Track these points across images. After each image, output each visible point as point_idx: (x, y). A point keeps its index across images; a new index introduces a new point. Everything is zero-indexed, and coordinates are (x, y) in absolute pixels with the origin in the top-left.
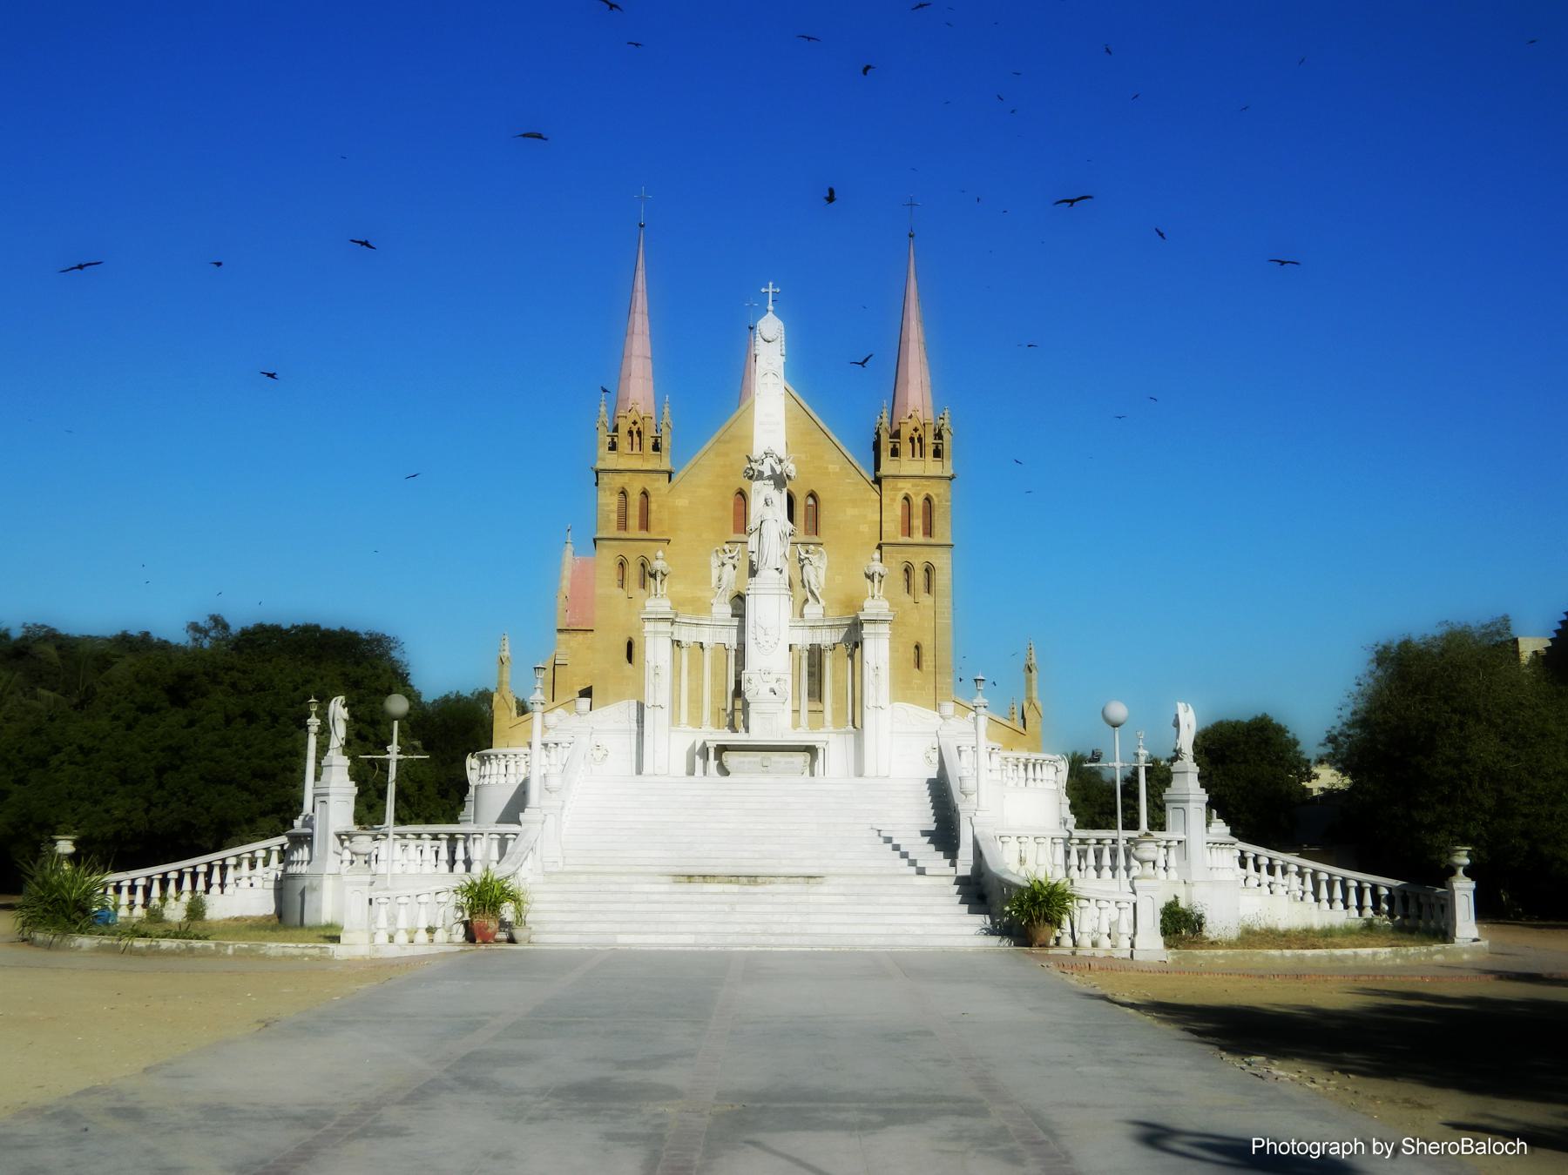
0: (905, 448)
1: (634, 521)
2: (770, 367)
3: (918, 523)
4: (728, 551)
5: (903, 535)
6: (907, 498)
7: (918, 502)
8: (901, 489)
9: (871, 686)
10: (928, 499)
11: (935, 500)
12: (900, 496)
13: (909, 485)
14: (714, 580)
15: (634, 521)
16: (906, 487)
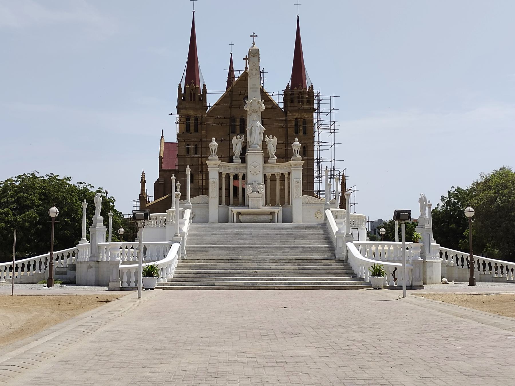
8: (295, 115)
9: (295, 189)
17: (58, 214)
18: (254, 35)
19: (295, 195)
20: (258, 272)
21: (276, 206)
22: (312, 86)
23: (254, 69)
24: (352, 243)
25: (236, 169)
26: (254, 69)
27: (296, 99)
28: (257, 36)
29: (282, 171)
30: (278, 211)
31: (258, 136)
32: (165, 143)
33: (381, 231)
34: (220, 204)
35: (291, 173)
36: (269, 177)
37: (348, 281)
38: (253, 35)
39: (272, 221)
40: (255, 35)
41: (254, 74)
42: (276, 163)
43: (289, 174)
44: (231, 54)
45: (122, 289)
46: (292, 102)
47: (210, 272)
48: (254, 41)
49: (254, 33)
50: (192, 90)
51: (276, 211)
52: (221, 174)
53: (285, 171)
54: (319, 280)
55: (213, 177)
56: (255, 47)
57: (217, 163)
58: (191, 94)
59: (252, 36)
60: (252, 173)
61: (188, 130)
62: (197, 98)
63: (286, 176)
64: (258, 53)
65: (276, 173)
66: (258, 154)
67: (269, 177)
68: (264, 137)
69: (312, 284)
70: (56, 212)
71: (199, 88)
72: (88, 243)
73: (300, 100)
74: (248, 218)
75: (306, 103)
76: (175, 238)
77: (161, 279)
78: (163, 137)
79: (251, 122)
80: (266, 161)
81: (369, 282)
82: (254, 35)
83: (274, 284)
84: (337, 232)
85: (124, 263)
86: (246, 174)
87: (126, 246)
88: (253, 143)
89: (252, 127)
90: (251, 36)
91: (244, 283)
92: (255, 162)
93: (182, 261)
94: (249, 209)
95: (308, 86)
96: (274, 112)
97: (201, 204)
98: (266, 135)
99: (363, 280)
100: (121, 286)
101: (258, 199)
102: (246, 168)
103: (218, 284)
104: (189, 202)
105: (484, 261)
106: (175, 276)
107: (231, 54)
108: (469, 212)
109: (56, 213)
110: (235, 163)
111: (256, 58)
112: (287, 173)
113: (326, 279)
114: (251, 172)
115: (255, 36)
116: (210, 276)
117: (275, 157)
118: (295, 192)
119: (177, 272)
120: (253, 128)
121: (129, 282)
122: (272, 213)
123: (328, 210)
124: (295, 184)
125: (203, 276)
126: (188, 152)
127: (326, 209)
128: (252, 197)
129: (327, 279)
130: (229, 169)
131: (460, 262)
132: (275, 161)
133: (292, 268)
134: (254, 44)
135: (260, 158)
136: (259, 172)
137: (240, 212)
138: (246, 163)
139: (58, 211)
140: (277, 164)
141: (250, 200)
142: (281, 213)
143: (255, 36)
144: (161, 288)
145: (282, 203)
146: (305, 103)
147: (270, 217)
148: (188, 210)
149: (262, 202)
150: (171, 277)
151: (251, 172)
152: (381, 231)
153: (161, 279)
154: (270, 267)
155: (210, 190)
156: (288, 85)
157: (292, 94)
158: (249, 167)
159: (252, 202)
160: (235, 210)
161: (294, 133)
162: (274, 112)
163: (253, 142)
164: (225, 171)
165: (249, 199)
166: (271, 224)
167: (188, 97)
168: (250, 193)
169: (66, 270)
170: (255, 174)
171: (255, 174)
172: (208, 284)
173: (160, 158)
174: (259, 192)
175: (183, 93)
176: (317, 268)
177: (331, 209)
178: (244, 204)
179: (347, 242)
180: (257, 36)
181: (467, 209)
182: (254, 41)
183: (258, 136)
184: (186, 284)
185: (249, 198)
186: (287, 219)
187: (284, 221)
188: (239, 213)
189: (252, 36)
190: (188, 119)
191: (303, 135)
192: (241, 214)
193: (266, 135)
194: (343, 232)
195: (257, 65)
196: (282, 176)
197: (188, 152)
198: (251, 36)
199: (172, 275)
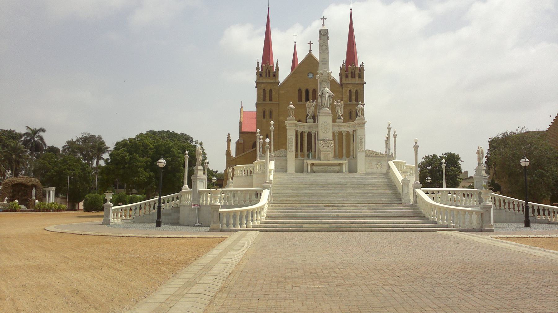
0: (350, 75)
1: (268, 98)
2: (324, 44)
3: (353, 97)
4: (312, 102)
5: (349, 101)
6: (350, 91)
7: (354, 91)
8: (349, 87)
9: (359, 144)
10: (357, 91)
11: (359, 91)
12: (348, 90)
13: (351, 86)
14: (307, 111)
15: (268, 98)
16: (350, 87)
17: (165, 164)
18: (324, 18)
19: (359, 149)
20: (339, 215)
21: (342, 158)
22: (363, 64)
23: (324, 46)
24: (420, 189)
25: (310, 127)
26: (324, 46)
27: (350, 75)
28: (326, 19)
29: (347, 129)
30: (344, 162)
31: (328, 101)
32: (244, 112)
33: (427, 179)
34: (297, 156)
35: (355, 131)
36: (336, 134)
37: (420, 224)
38: (323, 18)
39: (340, 171)
40: (324, 18)
41: (324, 49)
42: (343, 122)
43: (354, 131)
44: (295, 42)
45: (222, 230)
46: (347, 76)
47: (297, 215)
48: (323, 23)
49: (324, 17)
50: (268, 68)
51: (343, 162)
52: (297, 132)
53: (350, 129)
54: (395, 223)
55: (291, 135)
56: (325, 27)
57: (294, 123)
58: (266, 71)
59: (322, 19)
60: (323, 131)
61: (264, 99)
62: (271, 75)
63: (351, 134)
64: (327, 32)
66: (328, 115)
67: (336, 134)
68: (333, 102)
69: (390, 226)
70: (164, 163)
71: (273, 66)
72: (189, 190)
73: (353, 75)
75: (358, 78)
76: (265, 185)
77: (255, 221)
78: (242, 107)
79: (322, 89)
80: (334, 121)
81: (441, 225)
82: (324, 18)
83: (356, 227)
84: (403, 180)
85: (224, 207)
86: (318, 132)
88: (324, 106)
89: (323, 93)
90: (321, 19)
91: (329, 225)
92: (325, 122)
93: (271, 205)
95: (359, 63)
96: (333, 85)
98: (335, 100)
99: (435, 223)
100: (221, 228)
101: (328, 152)
102: (318, 127)
103: (306, 226)
104: (273, 155)
105: (538, 207)
106: (267, 219)
107: (295, 42)
108: (525, 163)
109: (163, 164)
110: (309, 122)
111: (326, 37)
112: (352, 131)
115: (325, 19)
116: (298, 219)
117: (342, 117)
118: (359, 147)
119: (268, 215)
120: (324, 94)
121: (228, 225)
122: (340, 165)
123: (390, 161)
124: (359, 140)
125: (291, 219)
126: (264, 117)
127: (388, 161)
128: (324, 151)
130: (304, 128)
131: (516, 208)
132: (342, 121)
133: (368, 212)
134: (323, 25)
135: (330, 119)
137: (313, 163)
138: (317, 123)
139: (165, 162)
140: (344, 123)
141: (322, 154)
142: (347, 164)
143: (325, 19)
144: (256, 230)
145: (348, 156)
146: (357, 78)
147: (337, 168)
148: (272, 161)
149: (331, 155)
150: (263, 219)
151: (322, 130)
152: (427, 179)
153: (256, 221)
154: (350, 211)
155: (289, 145)
156: (344, 64)
157: (347, 71)
158: (320, 125)
159: (323, 155)
160: (310, 162)
161: (348, 101)
162: (333, 85)
163: (324, 105)
164: (300, 130)
165: (320, 153)
166: (338, 174)
167: (264, 74)
169: (171, 212)
170: (325, 132)
172: (297, 226)
173: (241, 123)
174: (329, 147)
175: (260, 70)
176: (391, 212)
177: (393, 161)
178: (314, 157)
179: (416, 189)
180: (326, 19)
181: (523, 160)
182: (323, 23)
183: (328, 101)
184: (278, 226)
185: (321, 152)
186: (353, 169)
187: (350, 171)
188: (313, 165)
189: (322, 19)
190: (264, 90)
191: (356, 103)
192: (314, 165)
193: (335, 100)
194: (409, 180)
195: (326, 43)
196: (348, 133)
197: (264, 117)
198: (321, 19)
199: (264, 217)
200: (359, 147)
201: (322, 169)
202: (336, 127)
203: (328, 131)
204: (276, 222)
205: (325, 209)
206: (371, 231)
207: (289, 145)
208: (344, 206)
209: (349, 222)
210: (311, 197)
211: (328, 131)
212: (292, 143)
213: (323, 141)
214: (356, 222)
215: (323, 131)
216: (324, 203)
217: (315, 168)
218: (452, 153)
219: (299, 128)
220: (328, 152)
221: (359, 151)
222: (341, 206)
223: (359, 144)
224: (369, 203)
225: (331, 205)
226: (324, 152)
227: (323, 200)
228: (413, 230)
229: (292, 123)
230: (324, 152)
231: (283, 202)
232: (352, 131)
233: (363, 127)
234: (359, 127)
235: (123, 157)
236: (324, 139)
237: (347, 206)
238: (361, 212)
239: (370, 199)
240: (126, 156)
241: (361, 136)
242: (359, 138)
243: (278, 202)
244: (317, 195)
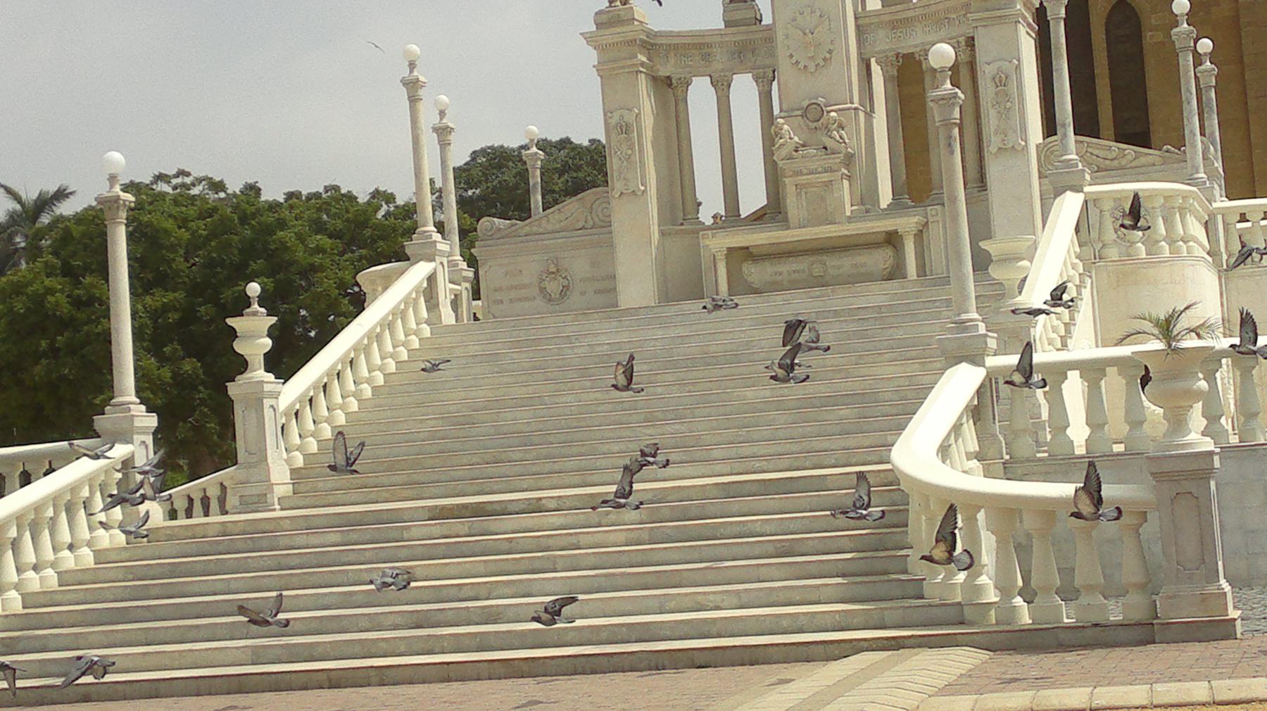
20: (418, 573)
39: (896, 272)
60: (797, 62)
65: (918, 49)
74: (786, 268)
87: (50, 462)
94: (788, 228)
97: (594, 231)
101: (825, 177)
112: (962, 39)
113: (711, 597)
114: (791, 56)
118: (992, 129)
128: (801, 173)
129: (718, 598)
136: (830, 52)
147: (881, 259)
151: (791, 56)
159: (799, 194)
168: (784, 152)
170: (812, 68)
171: (812, 68)
185: (787, 180)
200: (992, 129)
201: (794, 276)
202: (881, 33)
203: (825, 59)
204: (7, 646)
205: (406, 535)
206: (449, 680)
207: (615, 160)
208: (536, 507)
209: (399, 620)
210: (503, 456)
211: (825, 59)
212: (631, 148)
213: (802, 116)
214: (440, 617)
215: (797, 62)
216: (547, 484)
217: (755, 273)
218: (506, 145)
219: (672, 61)
220: (825, 177)
221: (993, 149)
222: (323, 522)
223: (992, 113)
224: (796, 464)
225: (465, 506)
226: (803, 179)
227: (556, 467)
228: (700, 658)
229: (618, 39)
230: (803, 179)
231: (331, 499)
232: (963, 43)
233: (1006, 12)
234: (987, 14)
235: (39, 300)
236: (805, 104)
237: (552, 505)
238: (573, 540)
239: (816, 444)
240: (49, 291)
241: (1000, 63)
242: (989, 76)
243: (307, 502)
244: (551, 439)
